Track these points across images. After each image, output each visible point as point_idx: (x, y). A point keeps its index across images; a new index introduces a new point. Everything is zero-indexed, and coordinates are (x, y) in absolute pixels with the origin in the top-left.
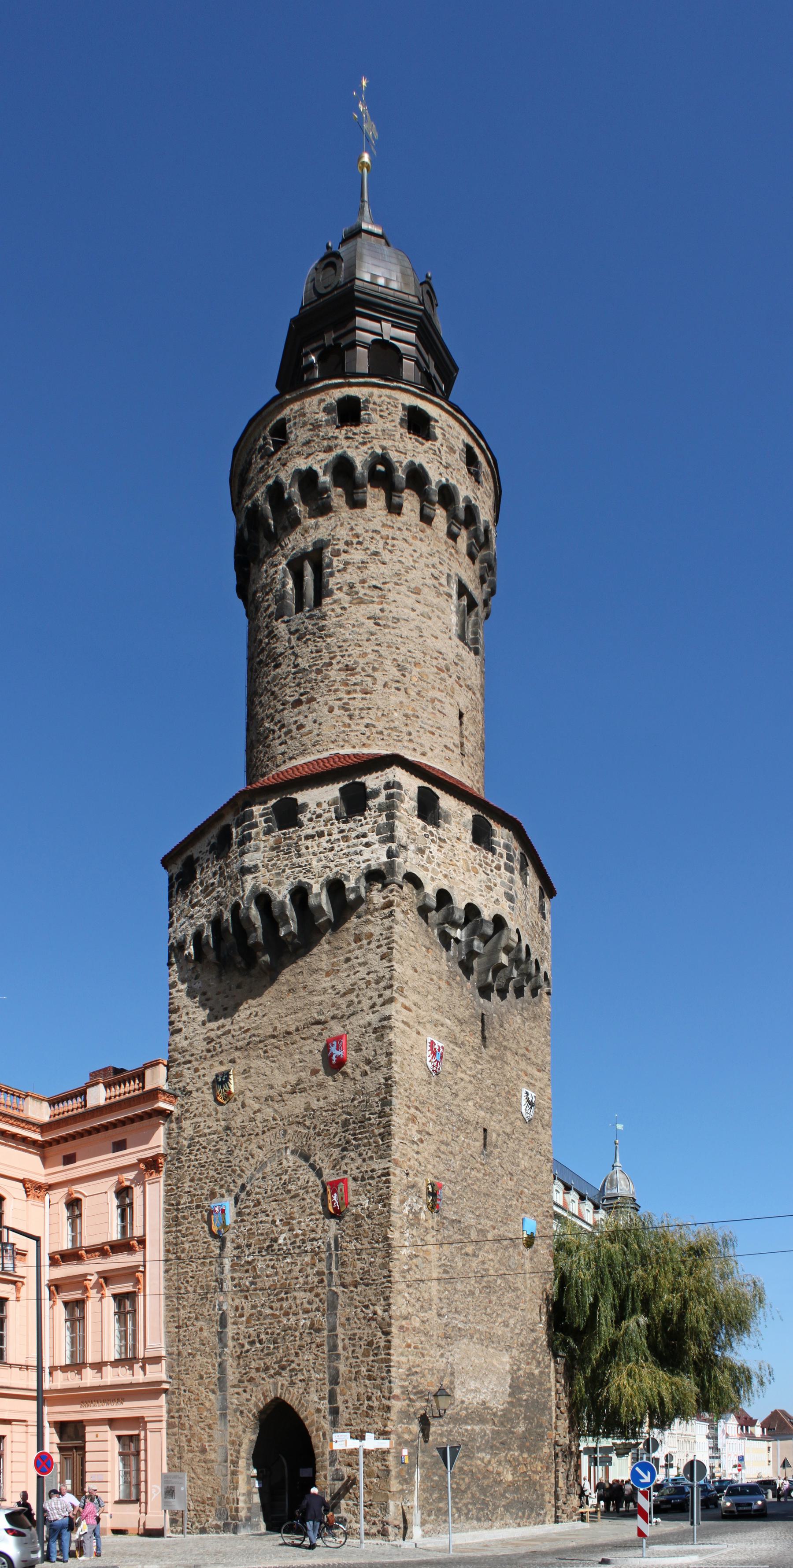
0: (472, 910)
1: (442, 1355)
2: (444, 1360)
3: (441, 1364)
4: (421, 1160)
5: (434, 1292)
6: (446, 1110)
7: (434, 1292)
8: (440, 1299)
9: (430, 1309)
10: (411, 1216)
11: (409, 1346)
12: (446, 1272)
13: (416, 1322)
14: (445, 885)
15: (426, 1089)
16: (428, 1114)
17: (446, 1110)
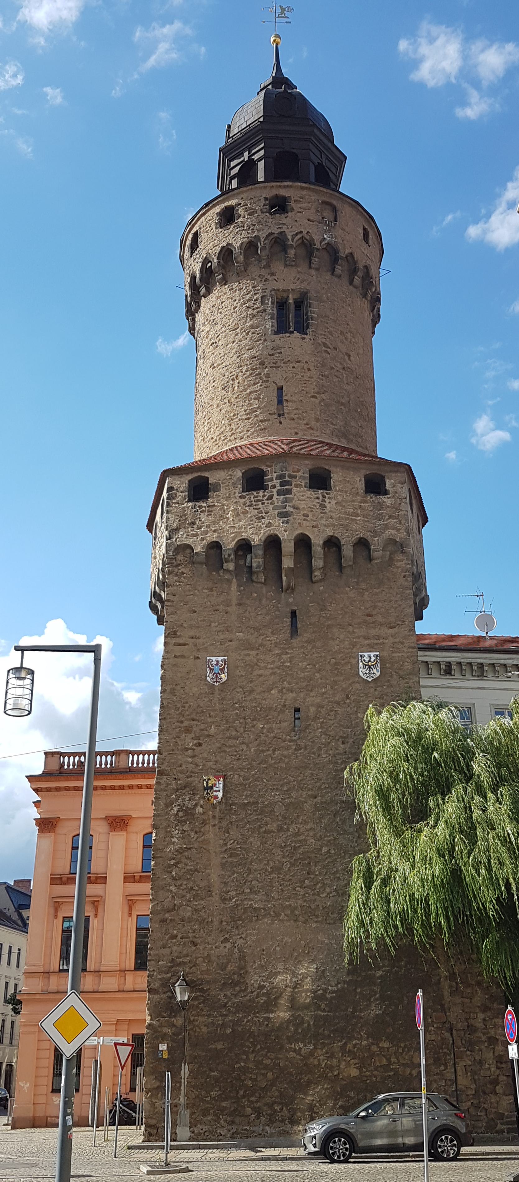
0: (244, 547)
1: (226, 940)
2: (229, 945)
3: (224, 949)
4: (197, 760)
5: (214, 878)
6: (236, 709)
7: (214, 878)
8: (226, 883)
9: (211, 896)
10: (180, 814)
11: (174, 937)
12: (231, 856)
13: (187, 912)
14: (212, 537)
15: (206, 700)
16: (209, 720)
17: (236, 709)
